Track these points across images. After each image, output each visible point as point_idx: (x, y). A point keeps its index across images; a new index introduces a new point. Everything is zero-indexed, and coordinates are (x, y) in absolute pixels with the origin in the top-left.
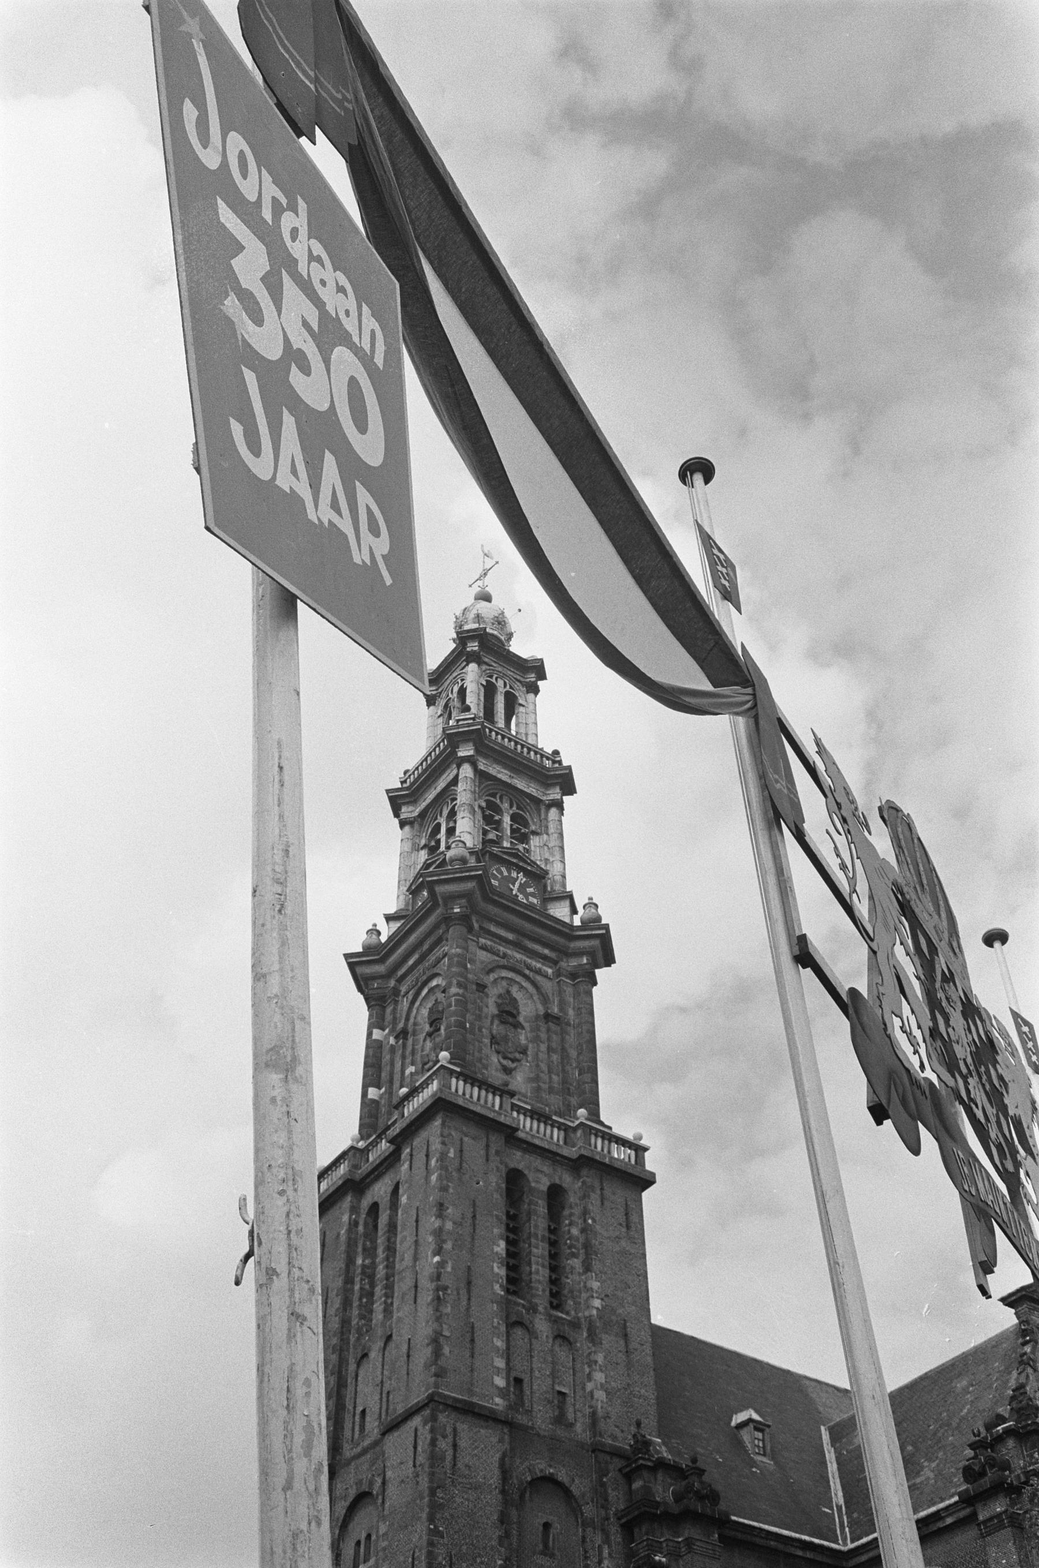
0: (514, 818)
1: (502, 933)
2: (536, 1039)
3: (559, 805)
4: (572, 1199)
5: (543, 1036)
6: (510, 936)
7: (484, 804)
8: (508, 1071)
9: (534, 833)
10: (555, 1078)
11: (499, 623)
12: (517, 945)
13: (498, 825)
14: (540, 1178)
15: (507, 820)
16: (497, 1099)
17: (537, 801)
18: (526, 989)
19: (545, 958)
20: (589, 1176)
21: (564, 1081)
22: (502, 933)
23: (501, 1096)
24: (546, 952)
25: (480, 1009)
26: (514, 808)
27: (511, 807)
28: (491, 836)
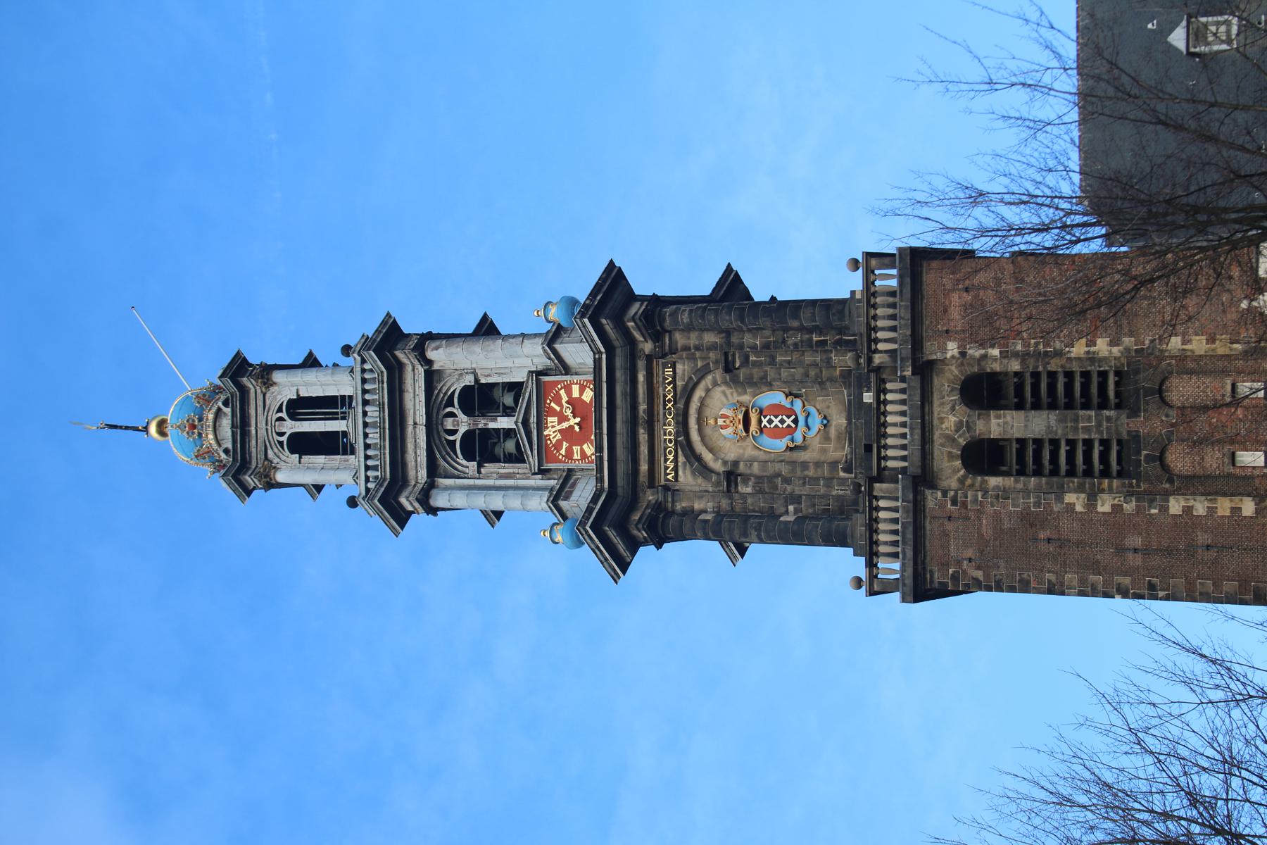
1: (644, 450)
5: (757, 373)
6: (643, 436)
9: (477, 380)
10: (808, 358)
11: (193, 427)
16: (882, 503)
17: (432, 377)
18: (703, 402)
22: (644, 450)
23: (877, 498)
24: (641, 377)
25: (759, 479)
26: (449, 409)
27: (452, 415)
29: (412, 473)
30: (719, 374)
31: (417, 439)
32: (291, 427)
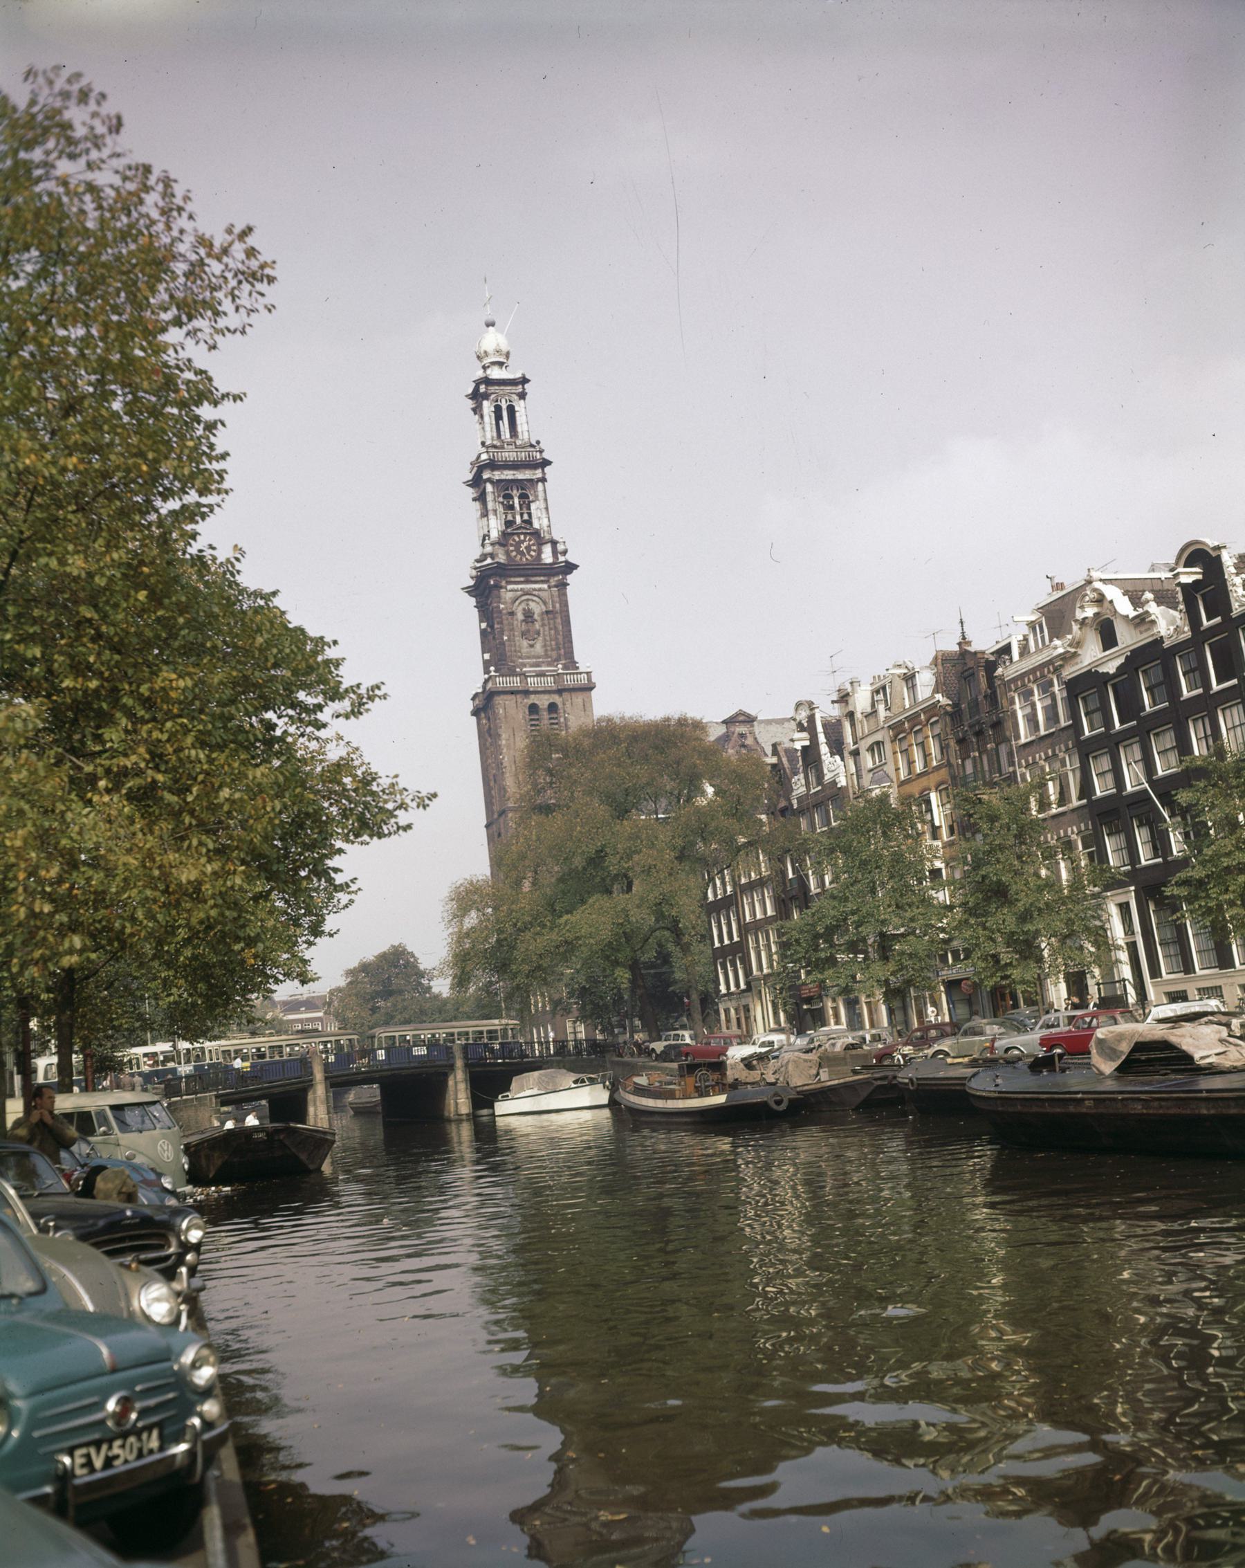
0: (520, 497)
2: (543, 625)
3: (543, 480)
4: (560, 706)
7: (501, 499)
8: (532, 646)
12: (527, 582)
13: (512, 507)
14: (543, 701)
15: (516, 500)
17: (531, 480)
19: (542, 582)
20: (566, 695)
21: (557, 644)
28: (510, 517)
29: (496, 473)
30: (544, 609)
31: (508, 475)
32: (504, 406)
